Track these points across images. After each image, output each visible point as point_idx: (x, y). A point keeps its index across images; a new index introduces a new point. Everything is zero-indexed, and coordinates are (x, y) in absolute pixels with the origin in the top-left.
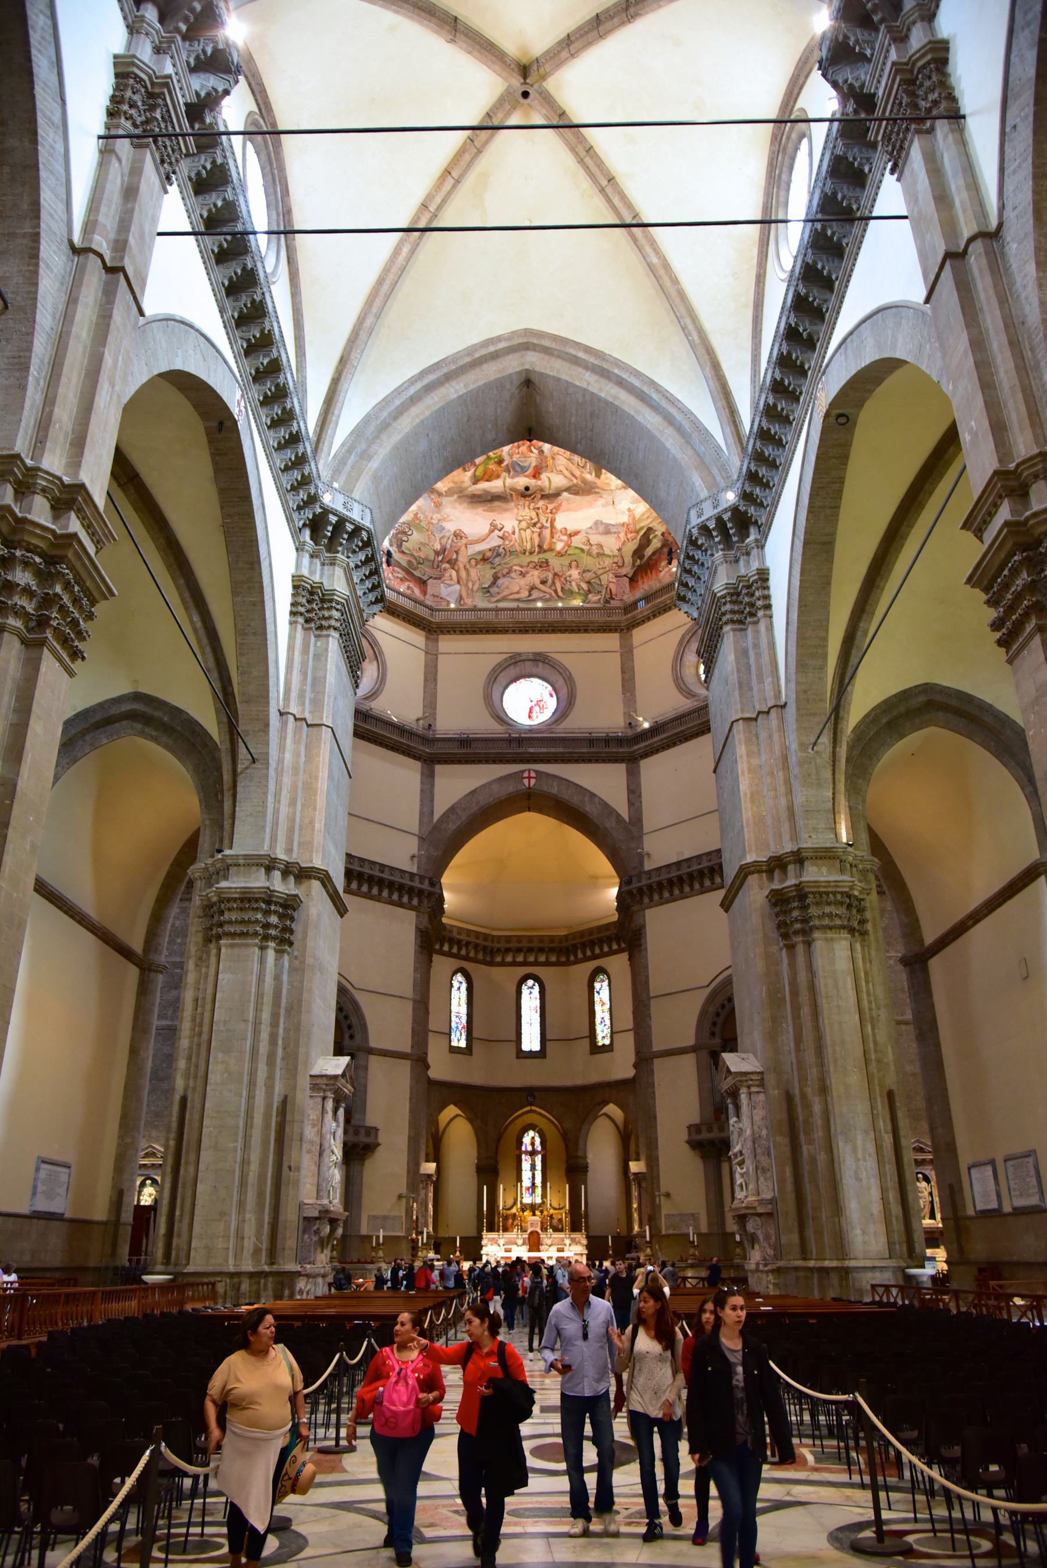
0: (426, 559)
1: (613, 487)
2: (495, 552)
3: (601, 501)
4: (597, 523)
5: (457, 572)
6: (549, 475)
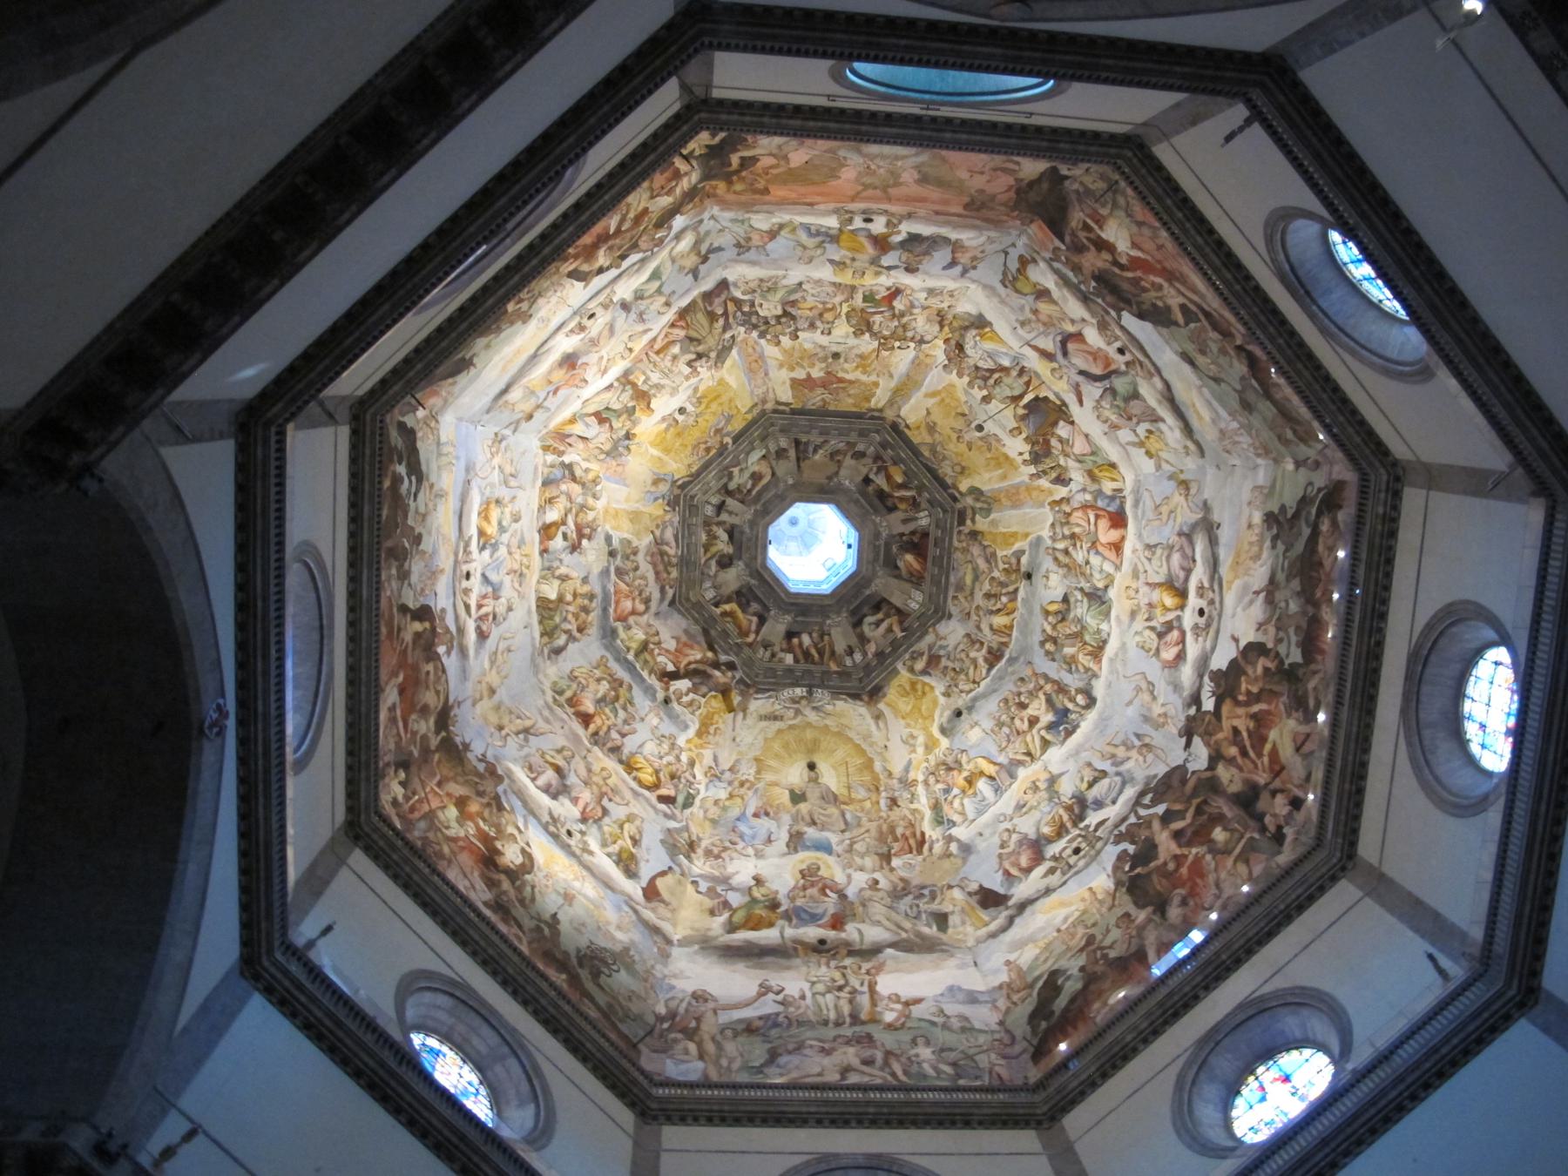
0: (638, 1018)
1: (971, 943)
2: (771, 1021)
3: (952, 962)
4: (951, 989)
5: (700, 1045)
6: (860, 926)
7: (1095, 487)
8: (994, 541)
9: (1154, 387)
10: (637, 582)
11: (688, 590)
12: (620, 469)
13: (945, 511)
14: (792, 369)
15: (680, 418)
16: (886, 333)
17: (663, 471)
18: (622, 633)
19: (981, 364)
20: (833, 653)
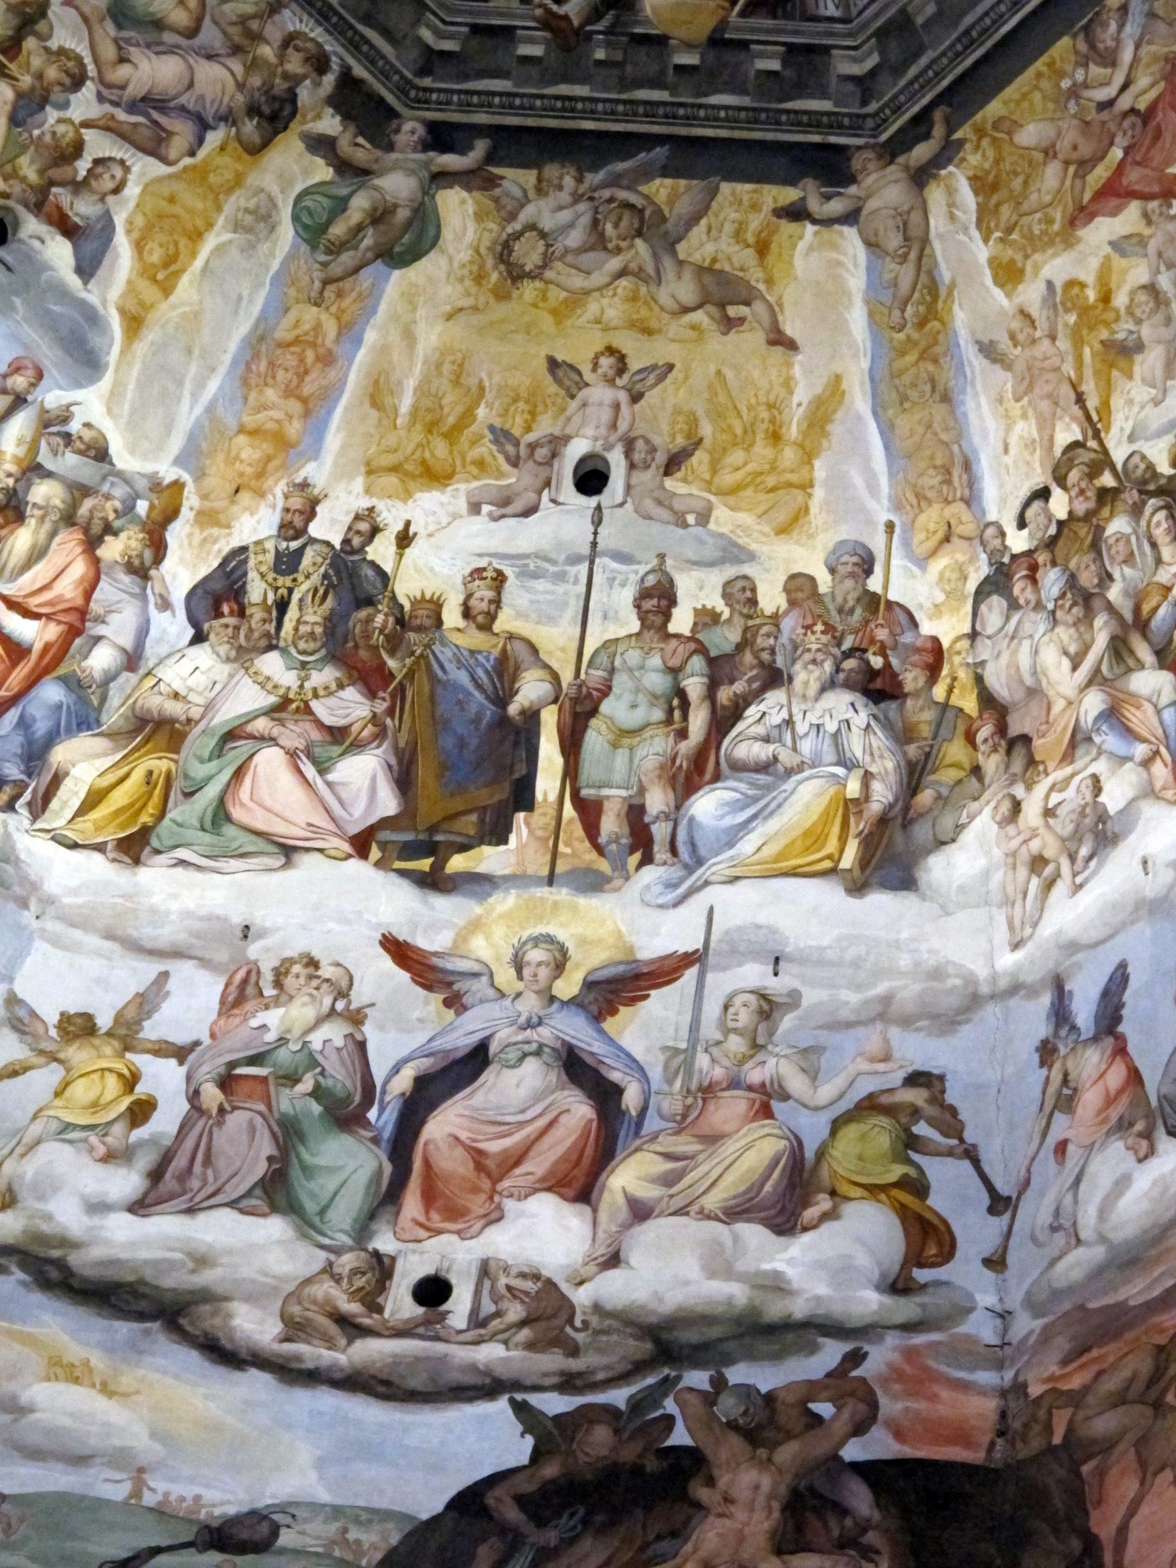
7: (114, 714)
8: (199, 175)
9: (256, 1295)
13: (431, 61)
16: (1118, 525)
19: (773, 706)
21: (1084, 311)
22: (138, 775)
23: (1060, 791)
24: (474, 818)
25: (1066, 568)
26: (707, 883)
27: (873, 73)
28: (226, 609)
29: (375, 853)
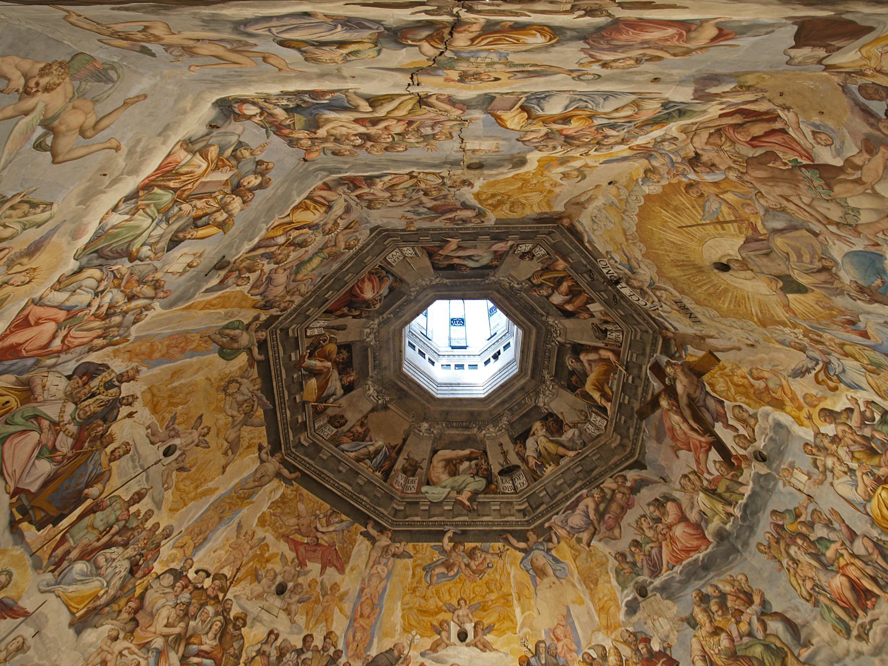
10: (650, 534)
11: (613, 452)
12: (559, 632)
13: (285, 331)
14: (335, 586)
15: (469, 627)
16: (210, 609)
17: (526, 579)
18: (715, 524)
20: (546, 270)
21: (262, 555)
22: (5, 399)
23: (129, 653)
24: (43, 514)
25: (191, 599)
26: (54, 592)
27: (303, 445)
28: (84, 378)
29: (14, 500)
